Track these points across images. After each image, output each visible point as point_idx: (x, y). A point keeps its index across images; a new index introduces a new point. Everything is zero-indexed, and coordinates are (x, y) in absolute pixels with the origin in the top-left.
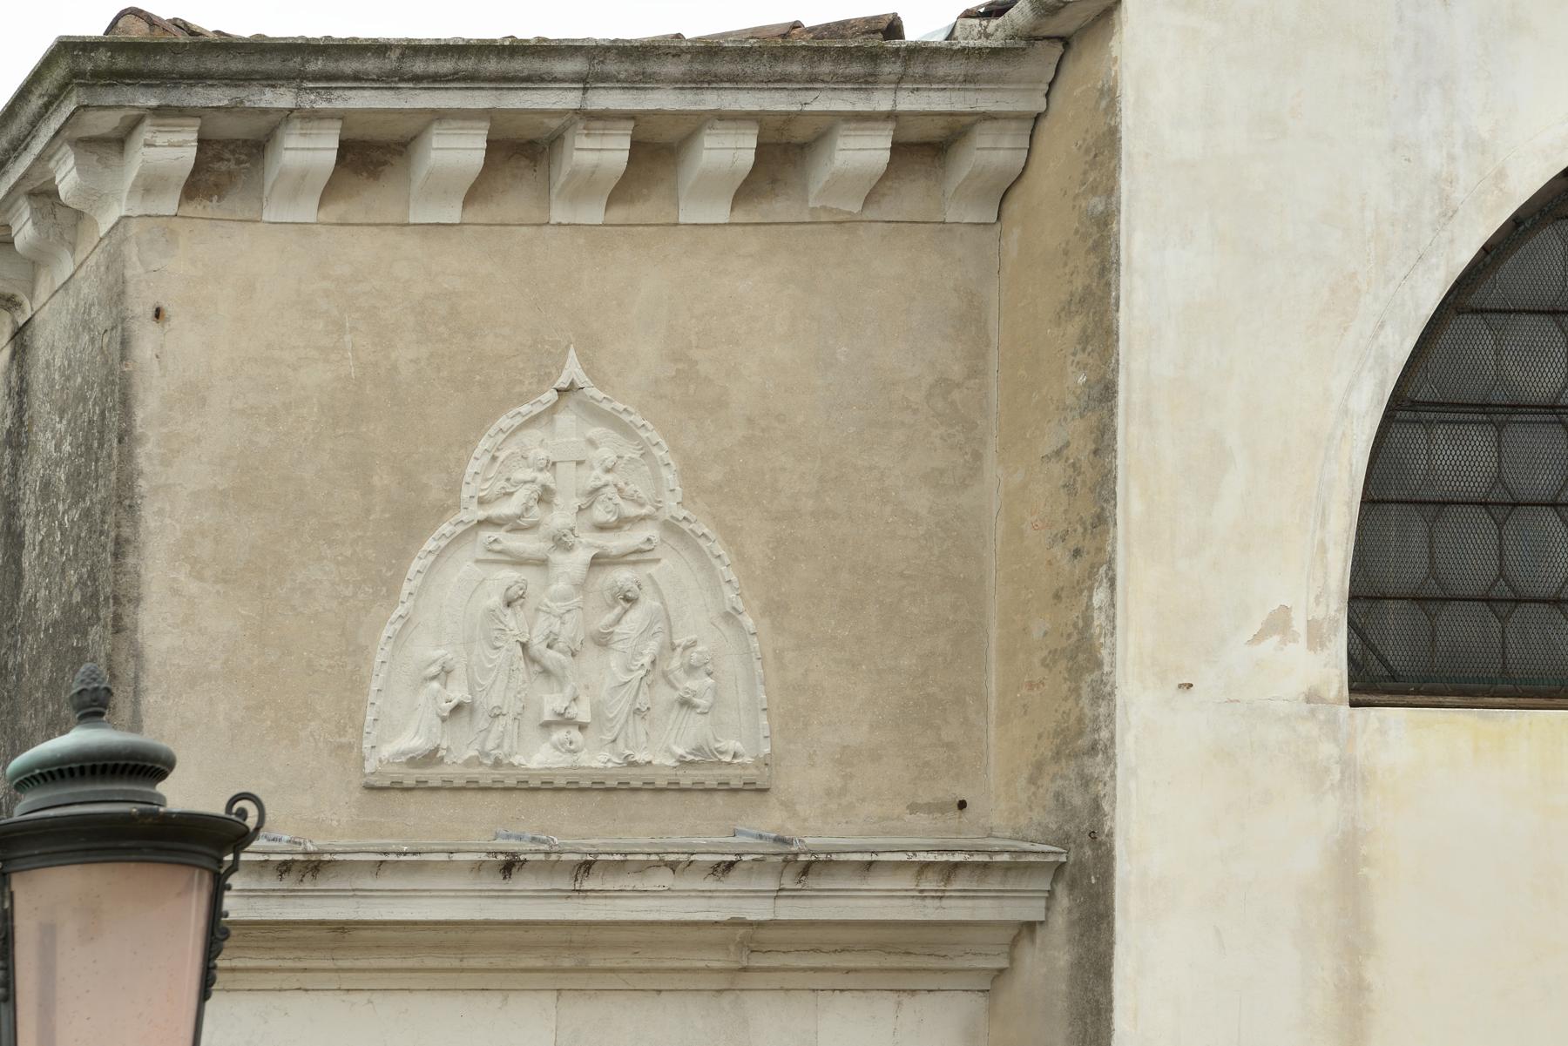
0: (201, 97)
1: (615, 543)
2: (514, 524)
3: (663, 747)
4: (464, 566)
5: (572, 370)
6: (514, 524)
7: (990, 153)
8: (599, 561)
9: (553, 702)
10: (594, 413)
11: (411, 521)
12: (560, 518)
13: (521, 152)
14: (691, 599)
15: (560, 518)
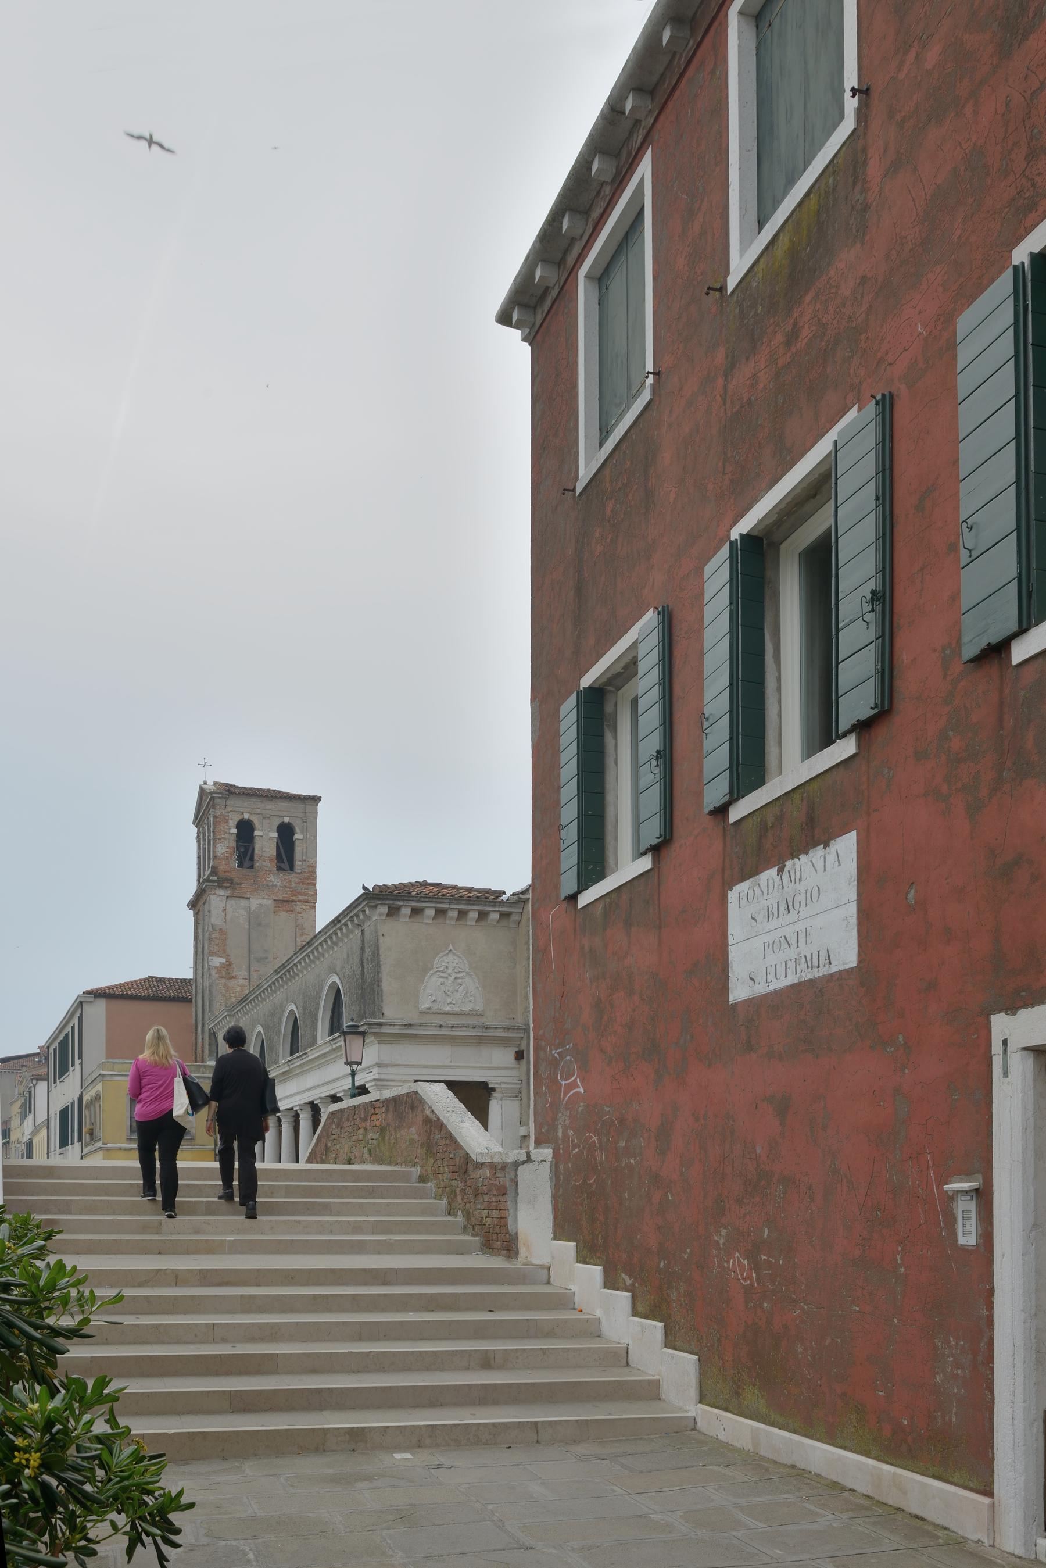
0: (387, 902)
1: (458, 975)
2: (442, 972)
3: (467, 1008)
4: (434, 978)
5: (451, 948)
6: (442, 972)
7: (515, 917)
8: (456, 978)
9: (449, 1000)
10: (454, 954)
11: (425, 970)
12: (449, 971)
13: (440, 913)
14: (471, 985)
15: (449, 971)
